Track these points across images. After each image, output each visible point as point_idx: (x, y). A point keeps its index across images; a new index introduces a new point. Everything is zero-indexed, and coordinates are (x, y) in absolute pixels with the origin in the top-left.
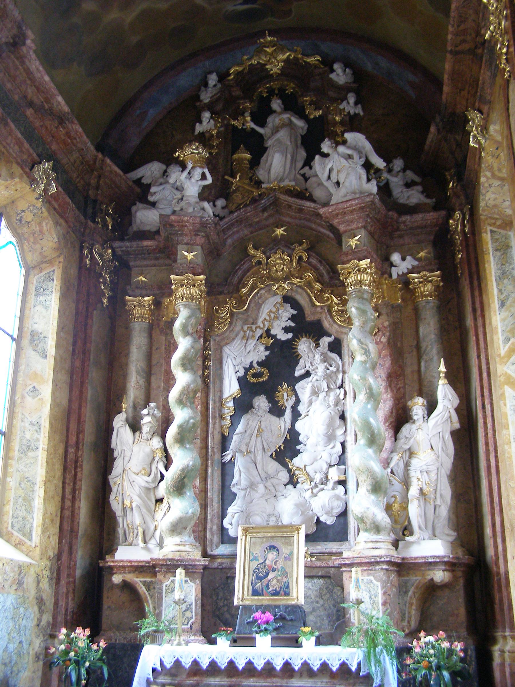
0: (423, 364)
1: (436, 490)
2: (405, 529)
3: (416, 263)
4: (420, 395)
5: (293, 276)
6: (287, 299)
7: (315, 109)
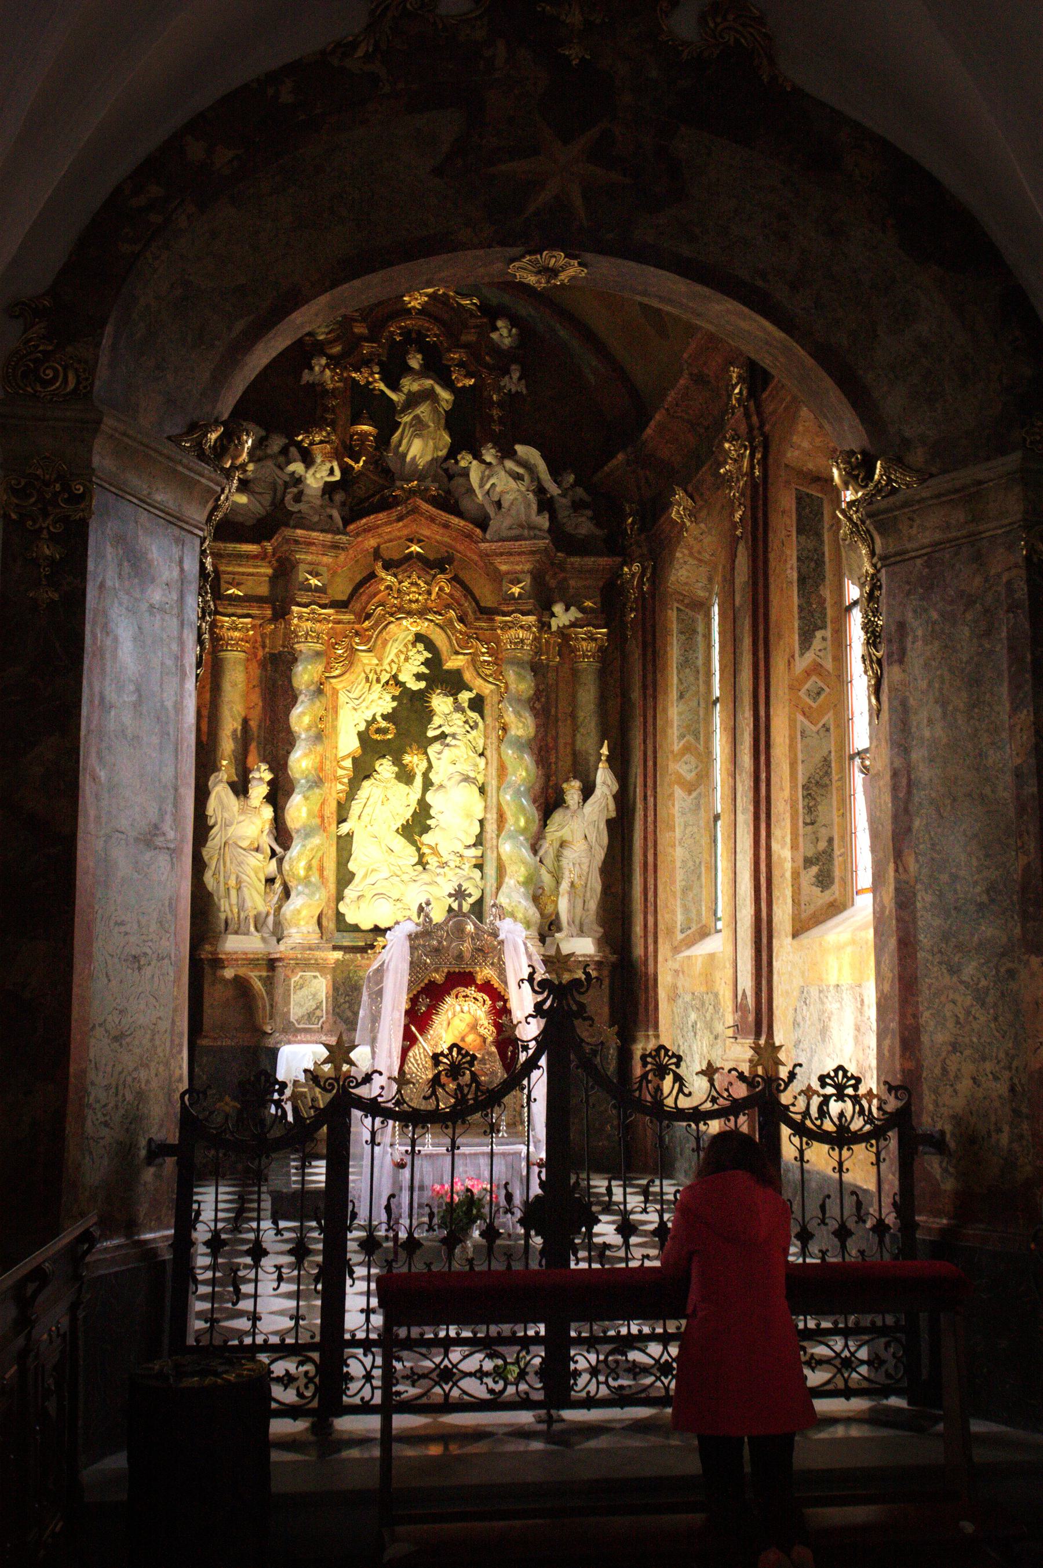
0: (578, 736)
1: (586, 884)
2: (551, 924)
3: (580, 615)
4: (575, 778)
5: (430, 610)
6: (419, 638)
7: (465, 376)
